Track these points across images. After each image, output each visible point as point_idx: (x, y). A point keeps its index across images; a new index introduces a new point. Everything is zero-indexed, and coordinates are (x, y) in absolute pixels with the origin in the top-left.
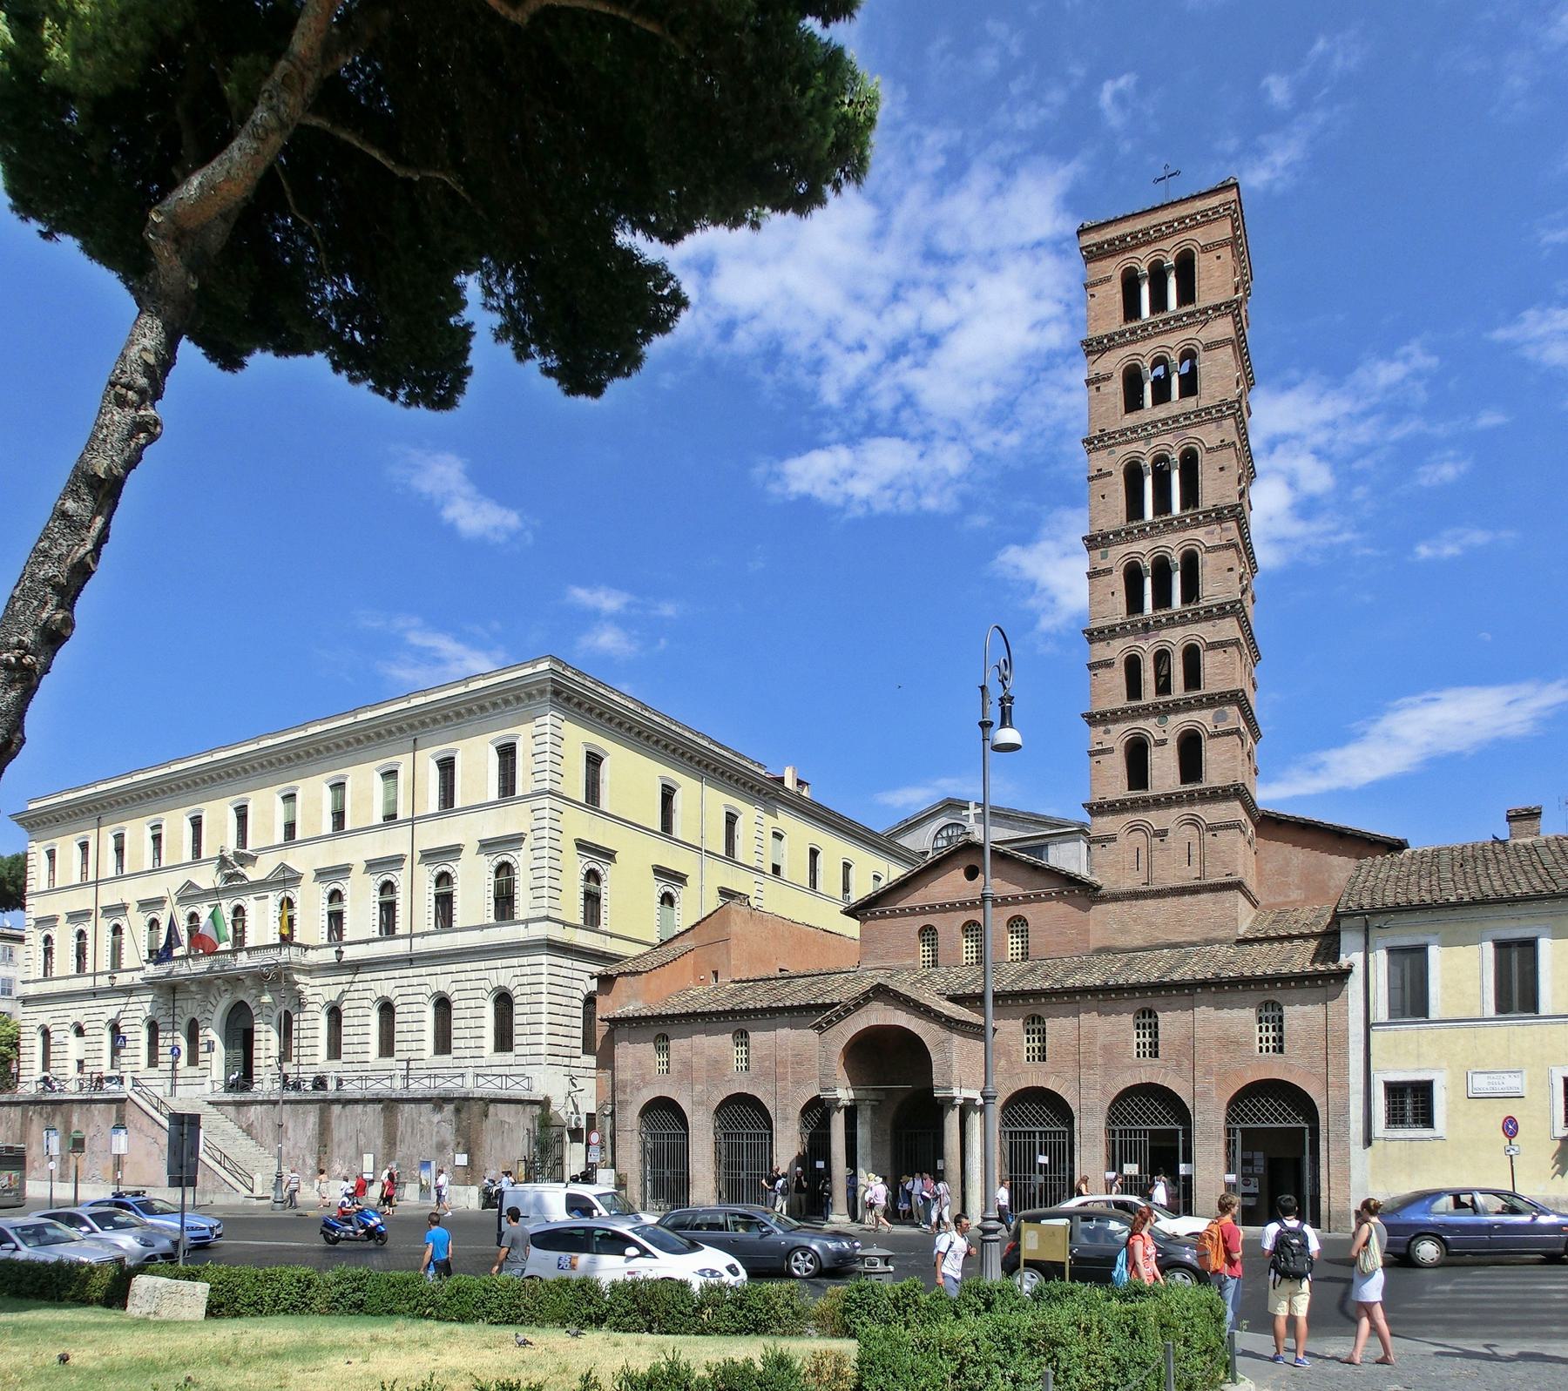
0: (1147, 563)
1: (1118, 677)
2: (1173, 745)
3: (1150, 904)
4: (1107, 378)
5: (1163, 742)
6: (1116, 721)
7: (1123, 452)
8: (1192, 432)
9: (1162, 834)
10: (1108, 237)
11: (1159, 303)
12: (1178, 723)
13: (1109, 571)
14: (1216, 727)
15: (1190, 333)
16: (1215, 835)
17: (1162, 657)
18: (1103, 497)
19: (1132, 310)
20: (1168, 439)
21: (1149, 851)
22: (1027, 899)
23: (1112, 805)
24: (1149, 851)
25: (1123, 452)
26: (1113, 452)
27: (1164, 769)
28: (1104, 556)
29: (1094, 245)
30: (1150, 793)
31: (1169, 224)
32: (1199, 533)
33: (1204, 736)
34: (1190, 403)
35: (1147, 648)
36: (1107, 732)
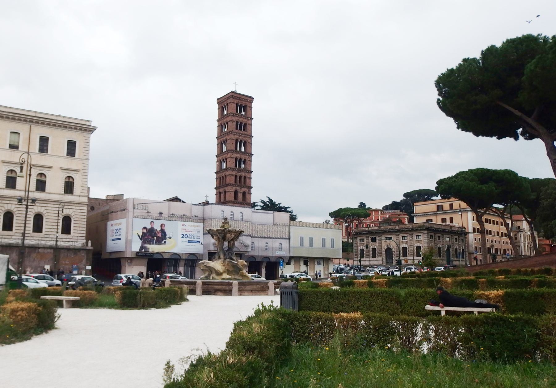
0: (239, 159)
1: (233, 178)
4: (234, 121)
5: (241, 193)
6: (234, 186)
7: (236, 136)
8: (247, 138)
11: (241, 111)
12: (243, 190)
13: (233, 158)
15: (246, 120)
17: (240, 177)
20: (243, 137)
23: (233, 202)
25: (236, 136)
28: (232, 154)
31: (245, 99)
32: (247, 157)
33: (247, 193)
34: (246, 133)
35: (239, 174)
36: (232, 188)
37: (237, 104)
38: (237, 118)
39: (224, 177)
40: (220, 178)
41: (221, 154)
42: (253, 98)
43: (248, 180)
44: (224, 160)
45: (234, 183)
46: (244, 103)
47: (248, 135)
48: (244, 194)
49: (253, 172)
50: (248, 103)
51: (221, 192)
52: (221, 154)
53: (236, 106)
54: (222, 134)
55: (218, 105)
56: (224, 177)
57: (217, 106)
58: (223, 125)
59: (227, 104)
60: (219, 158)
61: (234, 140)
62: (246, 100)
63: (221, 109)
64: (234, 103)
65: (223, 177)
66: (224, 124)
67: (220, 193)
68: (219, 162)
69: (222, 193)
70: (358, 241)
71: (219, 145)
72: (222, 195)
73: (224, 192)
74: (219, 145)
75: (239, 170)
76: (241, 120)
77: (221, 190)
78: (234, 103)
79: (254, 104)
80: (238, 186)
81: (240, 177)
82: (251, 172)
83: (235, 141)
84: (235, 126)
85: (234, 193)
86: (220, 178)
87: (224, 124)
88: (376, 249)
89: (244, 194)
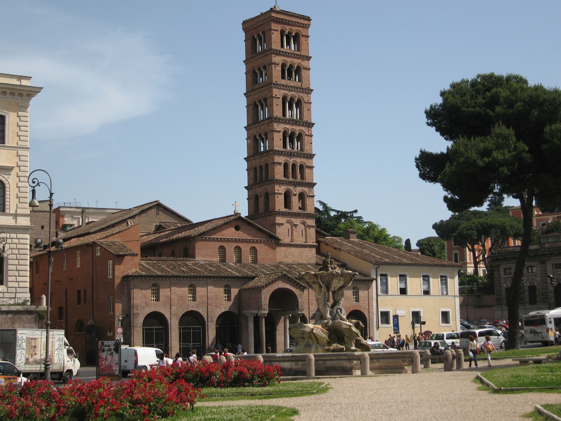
2: (297, 195)
3: (293, 249)
4: (278, 65)
9: (296, 226)
10: (280, 17)
14: (309, 193)
15: (299, 61)
16: (309, 229)
17: (294, 166)
18: (277, 105)
19: (282, 46)
21: (292, 231)
22: (257, 242)
24: (292, 231)
26: (280, 91)
27: (295, 202)
29: (275, 17)
30: (292, 211)
31: (295, 22)
37: (282, 32)
38: (283, 58)
39: (264, 168)
40: (256, 168)
41: (254, 123)
42: (308, 19)
43: (307, 171)
44: (263, 136)
45: (282, 178)
46: (295, 28)
47: (303, 89)
48: (302, 197)
49: (315, 157)
50: (300, 29)
51: (259, 194)
52: (254, 123)
53: (280, 35)
54: (256, 86)
55: (243, 34)
56: (264, 168)
57: (243, 35)
58: (257, 71)
59: (264, 33)
60: (251, 132)
61: (279, 98)
62: (298, 23)
63: (250, 41)
64: (277, 31)
65: (261, 167)
66: (259, 69)
67: (257, 197)
68: (252, 139)
69: (261, 197)
70: (502, 272)
71: (251, 106)
72: (262, 200)
73: (264, 194)
74: (251, 106)
75: (291, 155)
76: (289, 60)
77: (260, 190)
78: (277, 31)
79: (311, 31)
80: (290, 183)
81: (294, 166)
82: (311, 156)
83: (281, 100)
84: (280, 73)
85: (283, 196)
86: (256, 168)
87: (259, 69)
88: (537, 287)
89: (302, 197)
